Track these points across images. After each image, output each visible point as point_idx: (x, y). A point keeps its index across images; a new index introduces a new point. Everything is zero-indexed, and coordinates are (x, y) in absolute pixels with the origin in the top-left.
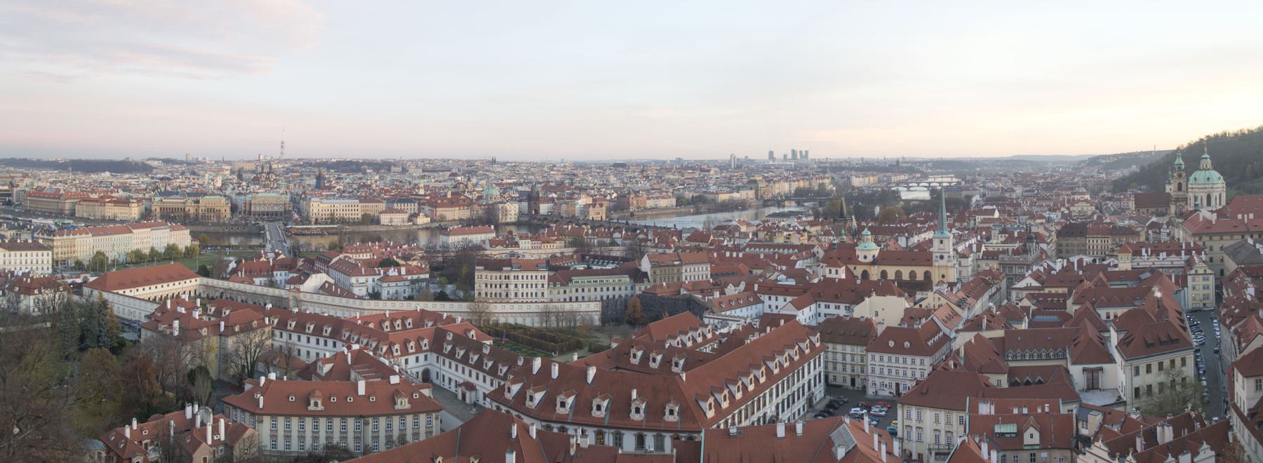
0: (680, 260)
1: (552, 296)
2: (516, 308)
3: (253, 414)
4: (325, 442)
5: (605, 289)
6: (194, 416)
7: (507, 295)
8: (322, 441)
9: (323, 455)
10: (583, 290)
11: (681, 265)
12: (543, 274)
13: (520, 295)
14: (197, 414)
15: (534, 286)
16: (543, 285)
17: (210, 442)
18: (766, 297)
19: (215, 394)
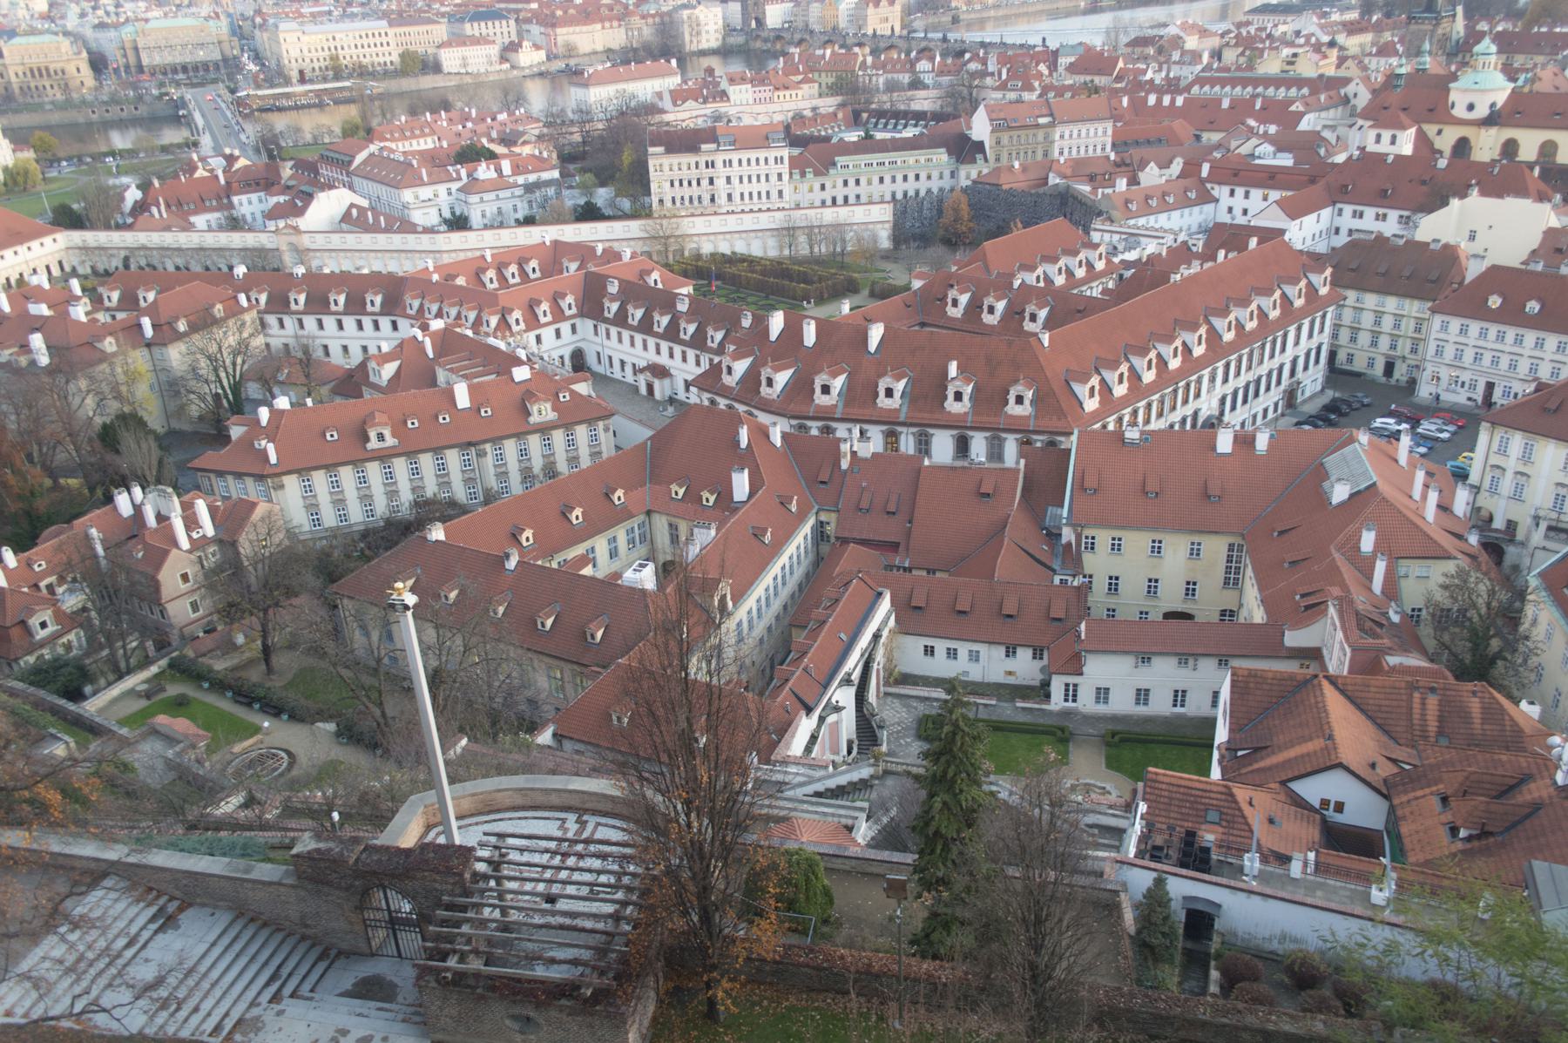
0: (1051, 115)
1: (798, 197)
2: (732, 223)
3: (260, 478)
4: (411, 497)
5: (899, 178)
6: (138, 509)
7: (713, 200)
8: (406, 496)
9: (412, 518)
10: (858, 182)
11: (1052, 125)
13: (736, 197)
14: (142, 503)
15: (763, 178)
16: (780, 176)
17: (185, 544)
18: (1226, 190)
19: (170, 460)
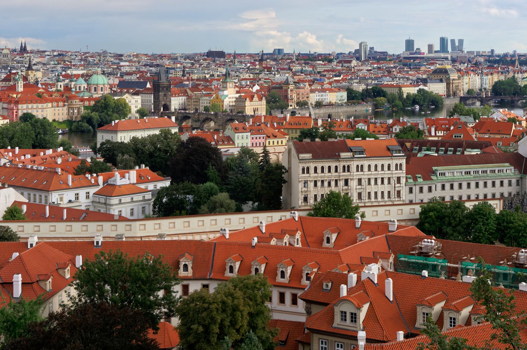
1: (412, 197)
10: (452, 187)
12: (399, 162)
13: (364, 196)
15: (386, 181)
16: (399, 179)
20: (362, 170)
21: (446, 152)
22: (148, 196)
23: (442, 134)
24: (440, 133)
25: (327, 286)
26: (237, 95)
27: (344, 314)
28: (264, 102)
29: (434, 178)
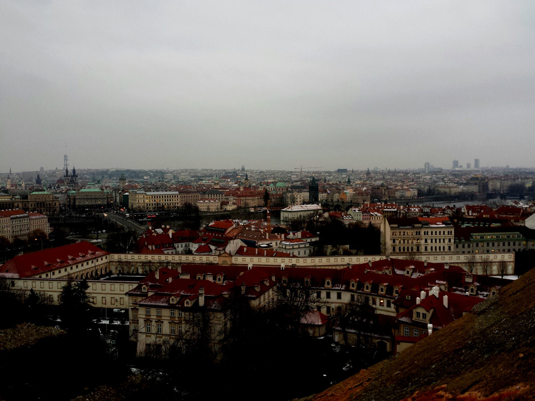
12: (450, 230)
15: (442, 241)
20: (427, 234)
21: (479, 224)
22: (308, 245)
23: (476, 215)
24: (475, 214)
25: (408, 297)
26: (354, 193)
27: (418, 314)
28: (369, 197)
29: (471, 239)
